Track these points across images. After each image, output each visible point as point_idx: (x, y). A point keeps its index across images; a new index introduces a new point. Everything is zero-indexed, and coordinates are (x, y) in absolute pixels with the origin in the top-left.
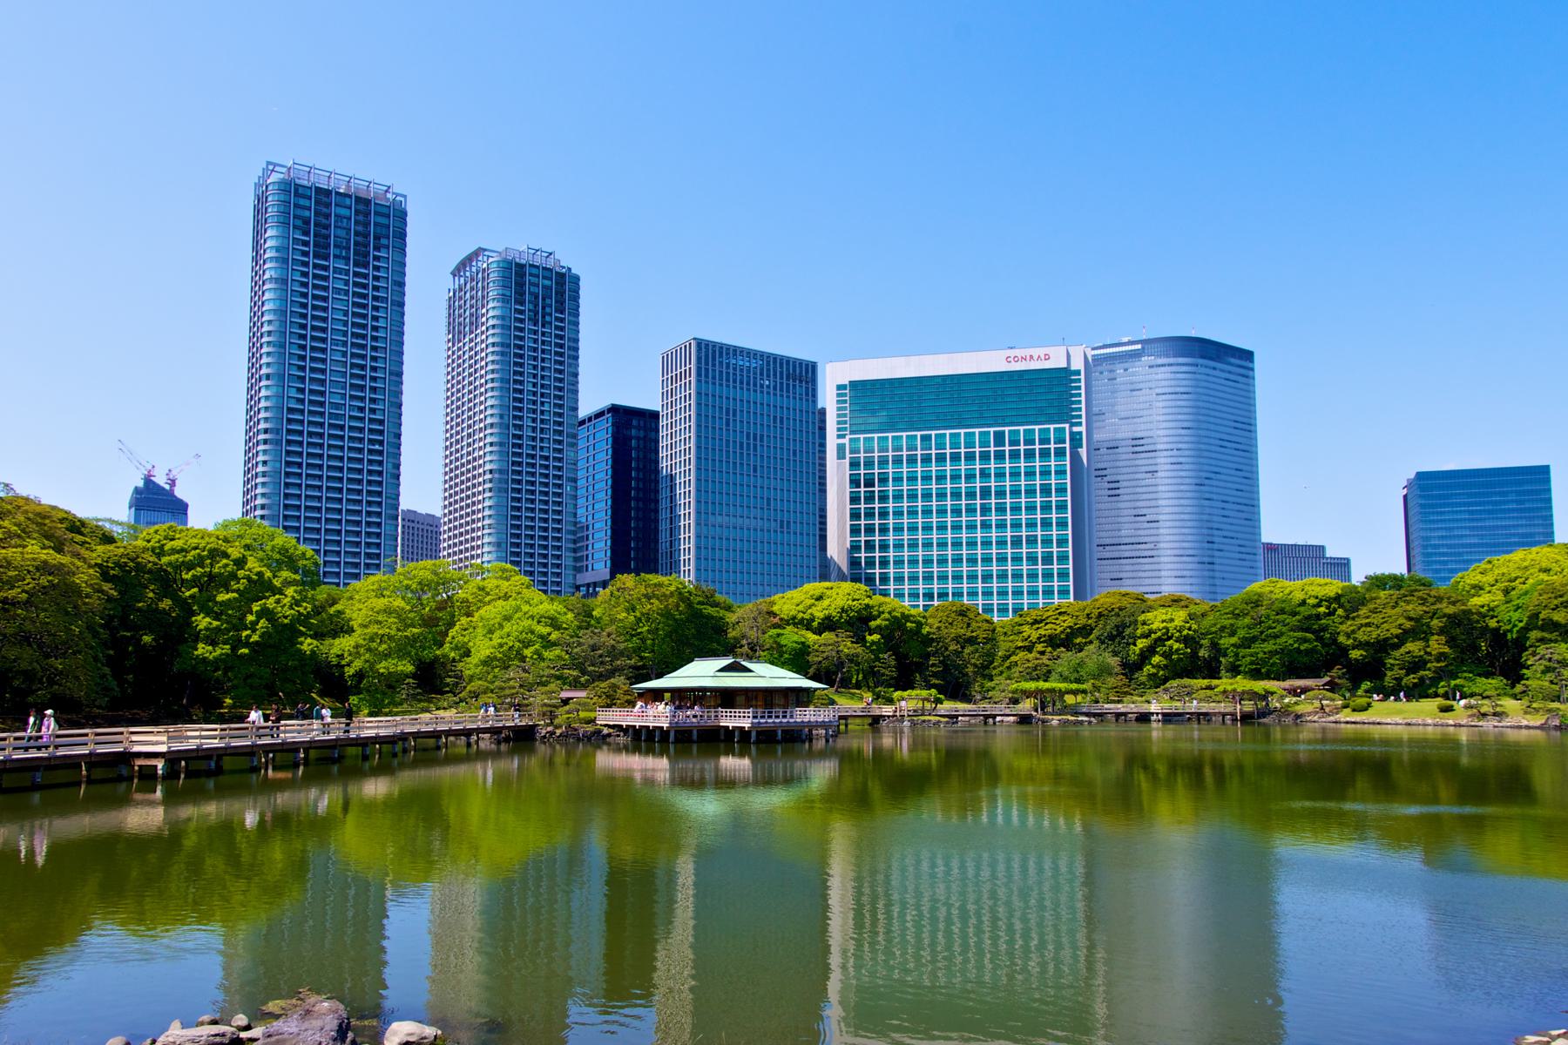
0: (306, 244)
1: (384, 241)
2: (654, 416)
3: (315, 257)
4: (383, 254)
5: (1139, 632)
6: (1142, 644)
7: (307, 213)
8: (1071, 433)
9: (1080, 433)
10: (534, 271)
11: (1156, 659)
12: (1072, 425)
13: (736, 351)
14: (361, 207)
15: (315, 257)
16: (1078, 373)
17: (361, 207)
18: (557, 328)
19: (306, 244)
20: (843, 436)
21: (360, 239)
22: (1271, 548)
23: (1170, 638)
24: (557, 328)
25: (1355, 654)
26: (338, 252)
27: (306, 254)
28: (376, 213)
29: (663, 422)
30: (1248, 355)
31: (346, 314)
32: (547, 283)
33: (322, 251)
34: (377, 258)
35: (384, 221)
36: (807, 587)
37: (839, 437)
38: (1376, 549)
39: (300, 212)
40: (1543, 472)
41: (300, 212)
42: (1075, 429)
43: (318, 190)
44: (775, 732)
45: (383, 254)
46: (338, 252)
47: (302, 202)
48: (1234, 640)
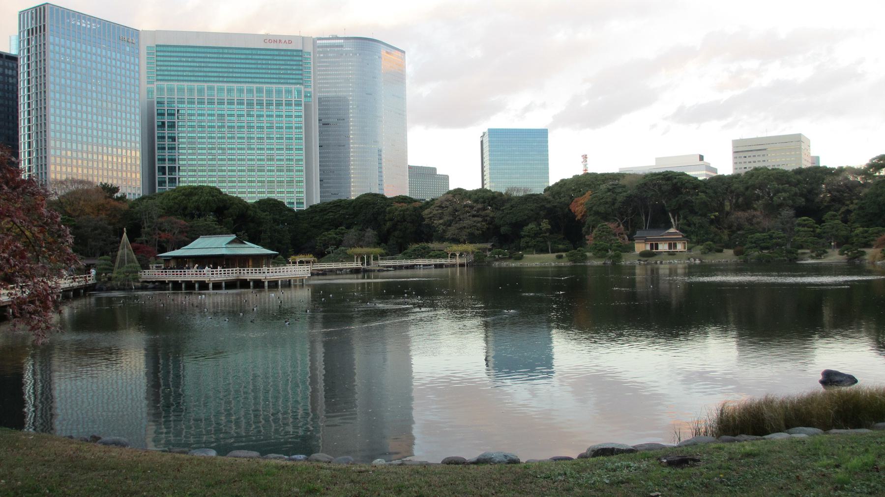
2: (14, 59)
5: (387, 218)
6: (388, 224)
8: (305, 92)
9: (310, 92)
11: (396, 233)
12: (306, 87)
13: (80, 16)
16: (309, 53)
20: (152, 83)
22: (410, 167)
23: (405, 221)
25: (503, 230)
29: (23, 62)
30: (404, 52)
37: (148, 83)
38: (465, 173)
40: (542, 134)
42: (309, 90)
44: (221, 283)
48: (441, 221)
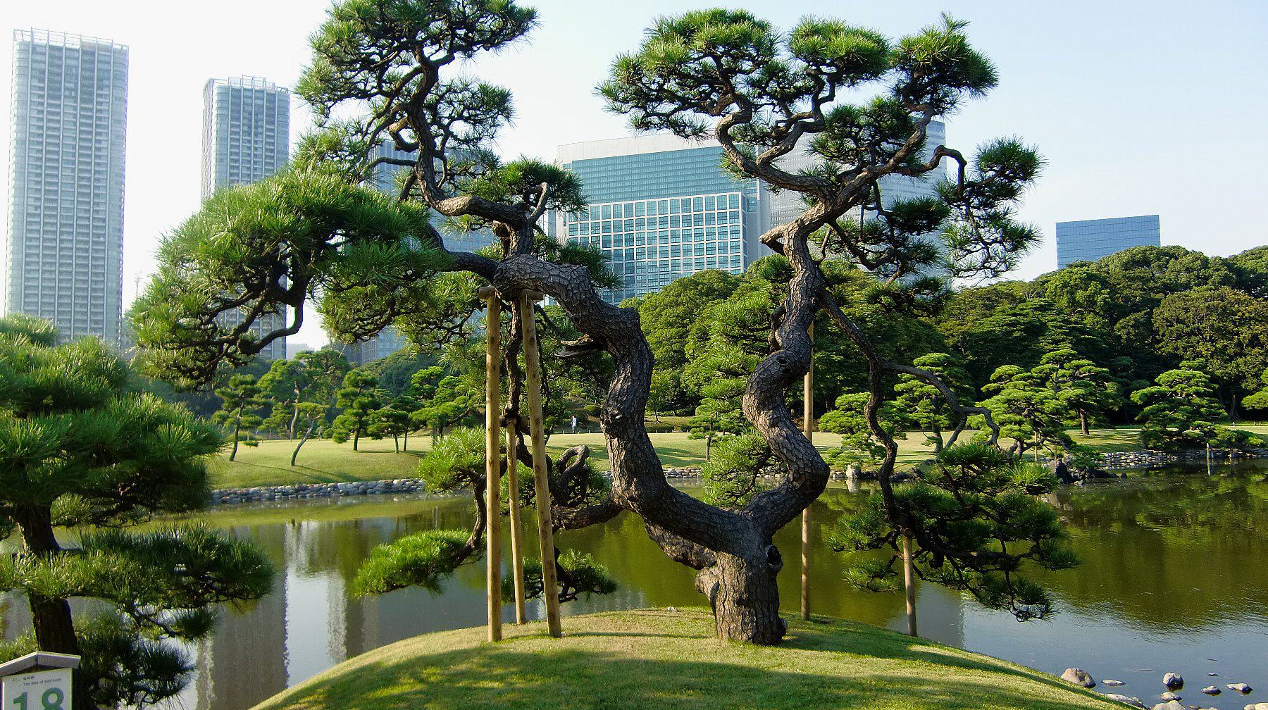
0: (42, 89)
1: (106, 82)
3: (50, 97)
4: (104, 92)
7: (42, 66)
10: (249, 94)
14: (87, 58)
15: (50, 97)
17: (87, 58)
18: (267, 136)
19: (42, 89)
21: (86, 82)
24: (267, 136)
26: (67, 93)
27: (42, 97)
28: (99, 62)
31: (74, 147)
32: (259, 102)
33: (54, 93)
34: (99, 96)
35: (105, 67)
36: (263, 377)
39: (36, 65)
41: (36, 65)
43: (52, 48)
45: (104, 92)
46: (67, 93)
47: (38, 58)
